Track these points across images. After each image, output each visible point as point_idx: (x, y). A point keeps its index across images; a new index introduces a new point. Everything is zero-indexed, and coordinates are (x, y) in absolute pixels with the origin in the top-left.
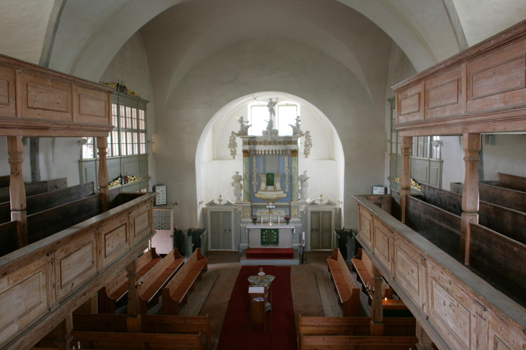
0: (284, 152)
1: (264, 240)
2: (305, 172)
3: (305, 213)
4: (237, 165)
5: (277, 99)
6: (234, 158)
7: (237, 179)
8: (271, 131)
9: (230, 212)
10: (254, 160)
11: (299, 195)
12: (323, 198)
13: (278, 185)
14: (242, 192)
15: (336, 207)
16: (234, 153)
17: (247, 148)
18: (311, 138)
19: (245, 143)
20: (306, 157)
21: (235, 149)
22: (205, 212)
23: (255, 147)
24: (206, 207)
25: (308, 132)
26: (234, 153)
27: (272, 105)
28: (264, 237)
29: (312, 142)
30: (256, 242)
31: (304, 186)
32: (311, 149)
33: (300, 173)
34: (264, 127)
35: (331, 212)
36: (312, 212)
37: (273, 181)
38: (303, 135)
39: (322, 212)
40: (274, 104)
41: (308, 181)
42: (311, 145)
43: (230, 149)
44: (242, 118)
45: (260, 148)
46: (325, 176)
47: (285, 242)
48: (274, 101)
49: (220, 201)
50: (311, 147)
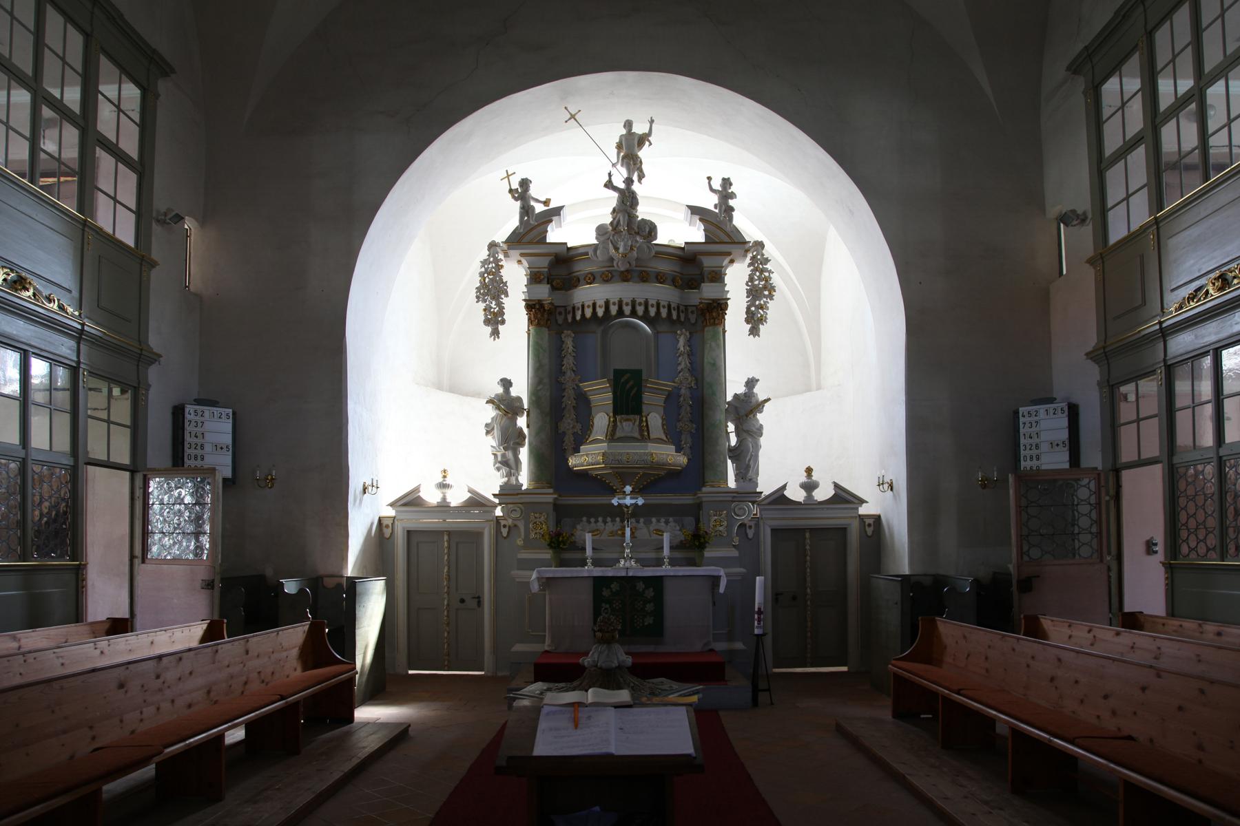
2: (751, 383)
4: (511, 357)
5: (652, 122)
6: (495, 333)
7: (506, 405)
8: (628, 224)
11: (730, 466)
12: (815, 477)
13: (655, 420)
14: (524, 453)
15: (863, 510)
16: (495, 320)
18: (768, 266)
19: (534, 278)
20: (754, 332)
21: (500, 305)
22: (387, 532)
24: (391, 512)
26: (495, 320)
27: (630, 149)
29: (776, 279)
31: (748, 432)
32: (771, 304)
33: (734, 387)
34: (604, 209)
35: (843, 531)
39: (814, 531)
40: (643, 140)
41: (761, 417)
42: (772, 289)
43: (482, 305)
44: (525, 183)
46: (826, 389)
48: (639, 128)
50: (771, 297)
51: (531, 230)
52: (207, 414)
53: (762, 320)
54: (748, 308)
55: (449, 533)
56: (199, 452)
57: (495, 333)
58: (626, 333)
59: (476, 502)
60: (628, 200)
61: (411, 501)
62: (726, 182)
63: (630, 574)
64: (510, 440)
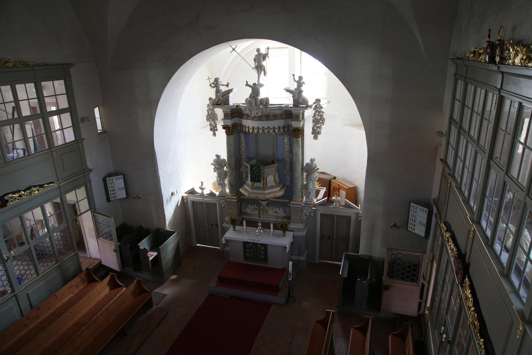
0: (282, 130)
1: (248, 254)
3: (312, 214)
4: (219, 145)
6: (214, 134)
9: (216, 204)
10: (243, 137)
17: (229, 122)
18: (322, 110)
19: (226, 116)
20: (315, 138)
21: (215, 123)
22: (185, 201)
23: (241, 121)
24: (186, 195)
25: (318, 101)
26: (214, 129)
28: (248, 250)
29: (325, 116)
30: (238, 256)
32: (323, 126)
33: (307, 161)
35: (350, 218)
36: (322, 215)
37: (259, 176)
38: (311, 107)
39: (337, 216)
40: (265, 57)
42: (323, 120)
43: (209, 123)
44: (216, 80)
45: (248, 123)
47: (274, 261)
48: (263, 51)
49: (202, 189)
50: (323, 123)
51: (221, 99)
52: (114, 179)
53: (319, 133)
54: (313, 128)
55: (206, 203)
56: (114, 192)
57: (214, 134)
58: (261, 140)
59: (212, 194)
60: (255, 89)
61: (192, 192)
62: (300, 78)
63: (255, 242)
64: (221, 176)
